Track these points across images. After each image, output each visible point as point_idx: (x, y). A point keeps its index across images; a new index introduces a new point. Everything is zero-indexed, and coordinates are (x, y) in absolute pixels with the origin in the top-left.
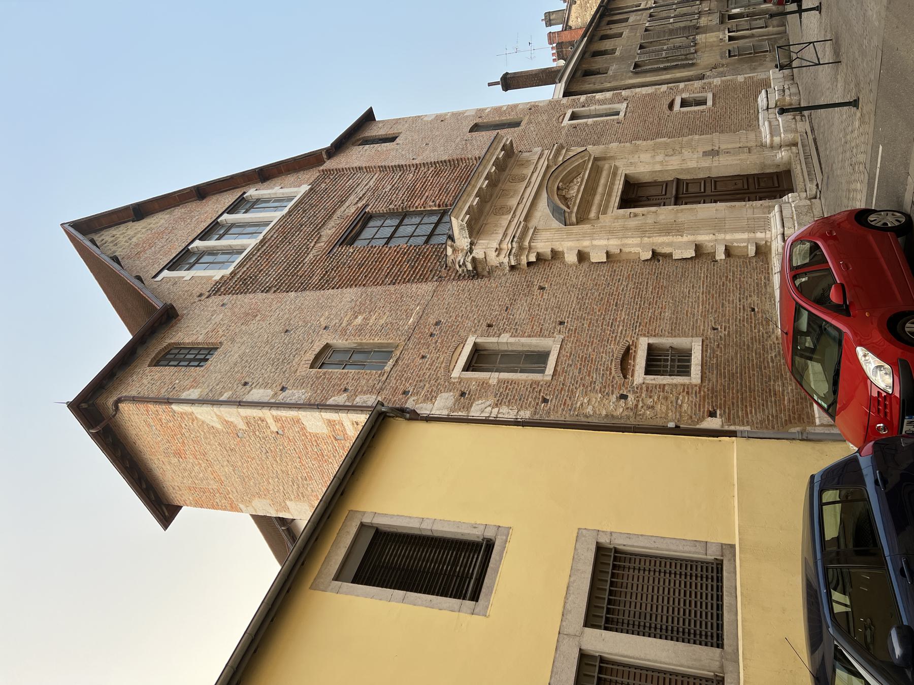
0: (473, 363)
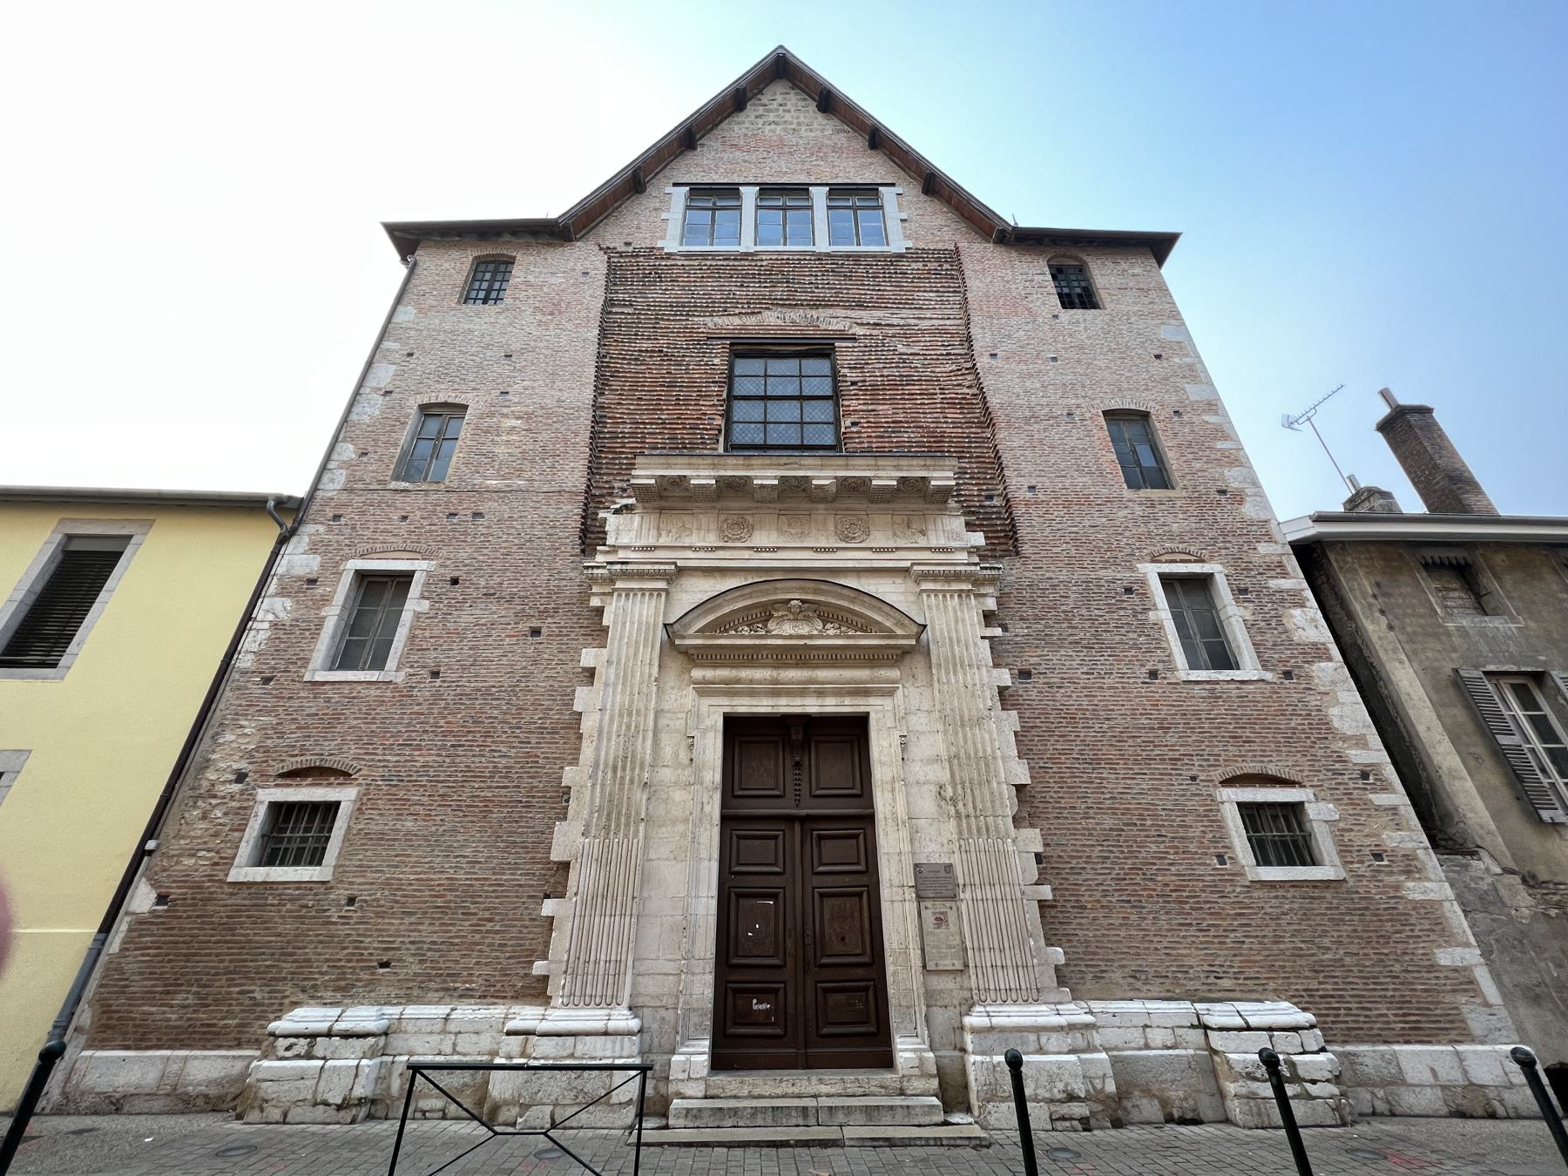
0: (397, 580)
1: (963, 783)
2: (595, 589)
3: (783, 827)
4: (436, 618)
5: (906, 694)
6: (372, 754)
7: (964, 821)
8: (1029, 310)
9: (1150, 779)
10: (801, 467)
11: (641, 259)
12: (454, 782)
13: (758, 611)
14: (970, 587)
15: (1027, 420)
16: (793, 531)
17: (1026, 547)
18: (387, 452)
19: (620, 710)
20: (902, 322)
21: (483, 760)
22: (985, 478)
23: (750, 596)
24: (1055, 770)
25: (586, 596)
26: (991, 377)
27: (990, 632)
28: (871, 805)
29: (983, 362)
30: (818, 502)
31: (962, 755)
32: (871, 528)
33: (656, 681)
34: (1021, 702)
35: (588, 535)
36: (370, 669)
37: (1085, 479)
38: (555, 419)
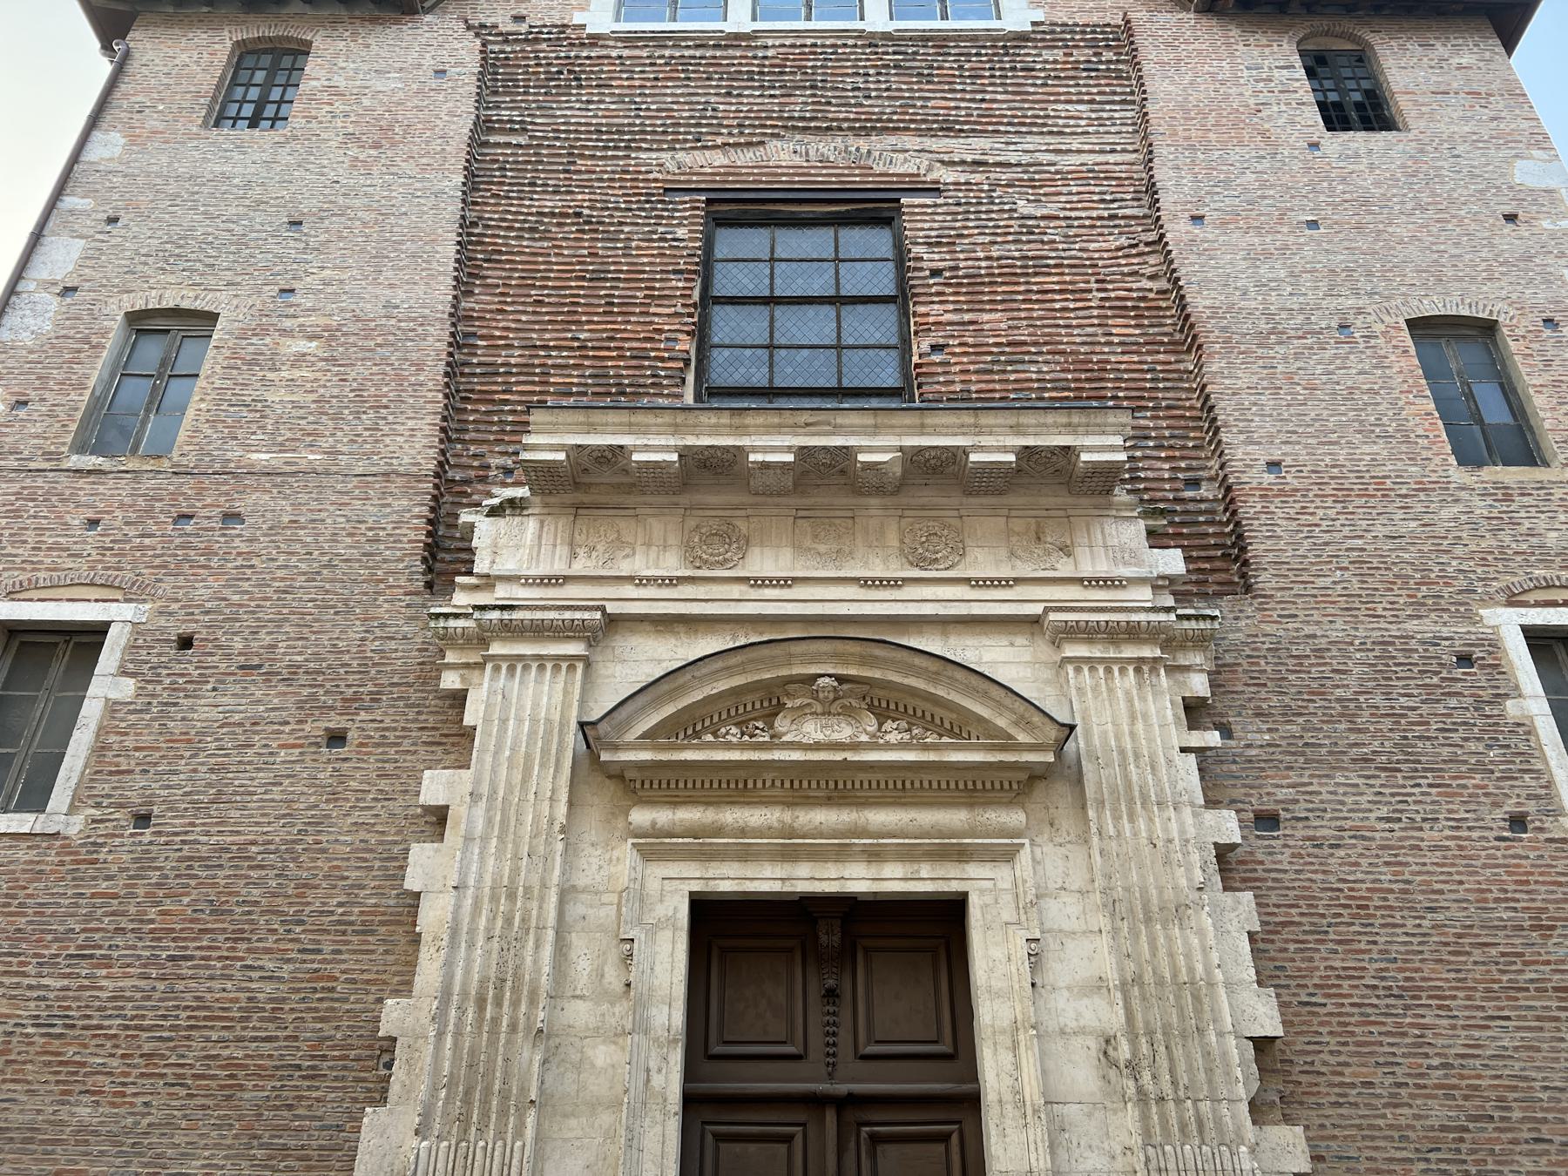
0: (76, 639)
1: (1150, 1033)
2: (451, 657)
3: (802, 1118)
4: (147, 711)
5: (1038, 855)
6: (17, 974)
7: (1154, 1109)
8: (1263, 134)
9: (1518, 1028)
10: (837, 430)
11: (544, 46)
12: (173, 1028)
13: (756, 697)
14: (1158, 653)
15: (1262, 339)
16: (822, 548)
17: (1264, 576)
18: (61, 399)
19: (492, 888)
20: (1026, 159)
21: (229, 985)
22: (1184, 447)
23: (742, 669)
24: (1330, 1008)
25: (432, 669)
26: (1193, 258)
27: (1197, 739)
28: (972, 1074)
29: (1177, 230)
30: (870, 495)
31: (1148, 977)
32: (968, 542)
33: (562, 831)
34: (1260, 874)
35: (441, 555)
36: (19, 809)
37: (1375, 448)
38: (379, 340)
